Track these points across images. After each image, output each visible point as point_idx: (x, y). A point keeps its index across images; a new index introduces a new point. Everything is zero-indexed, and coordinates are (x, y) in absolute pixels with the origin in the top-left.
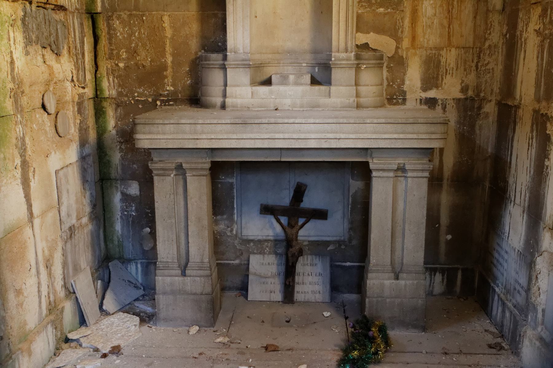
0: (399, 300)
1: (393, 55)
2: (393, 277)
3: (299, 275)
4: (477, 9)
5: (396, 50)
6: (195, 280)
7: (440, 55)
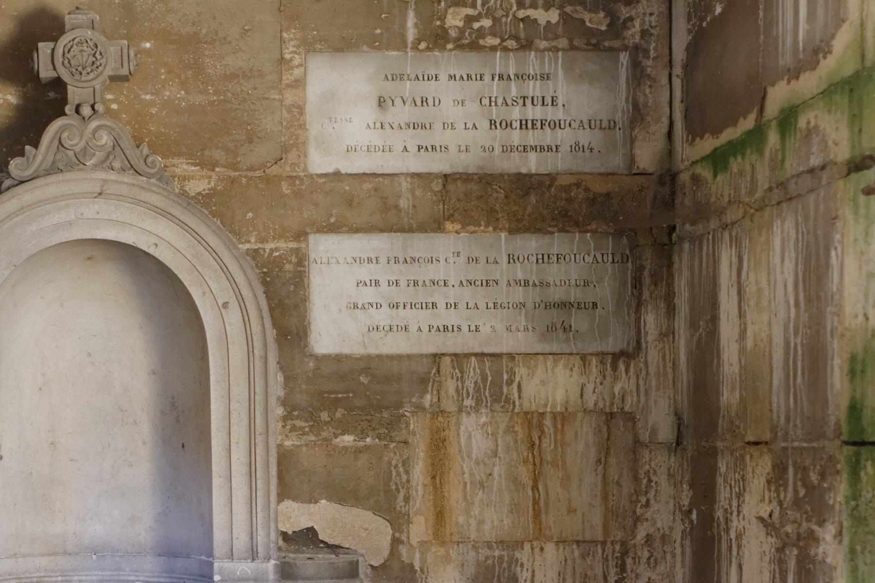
1: (386, 561)
4: (608, 439)
5: (392, 549)
7: (513, 561)
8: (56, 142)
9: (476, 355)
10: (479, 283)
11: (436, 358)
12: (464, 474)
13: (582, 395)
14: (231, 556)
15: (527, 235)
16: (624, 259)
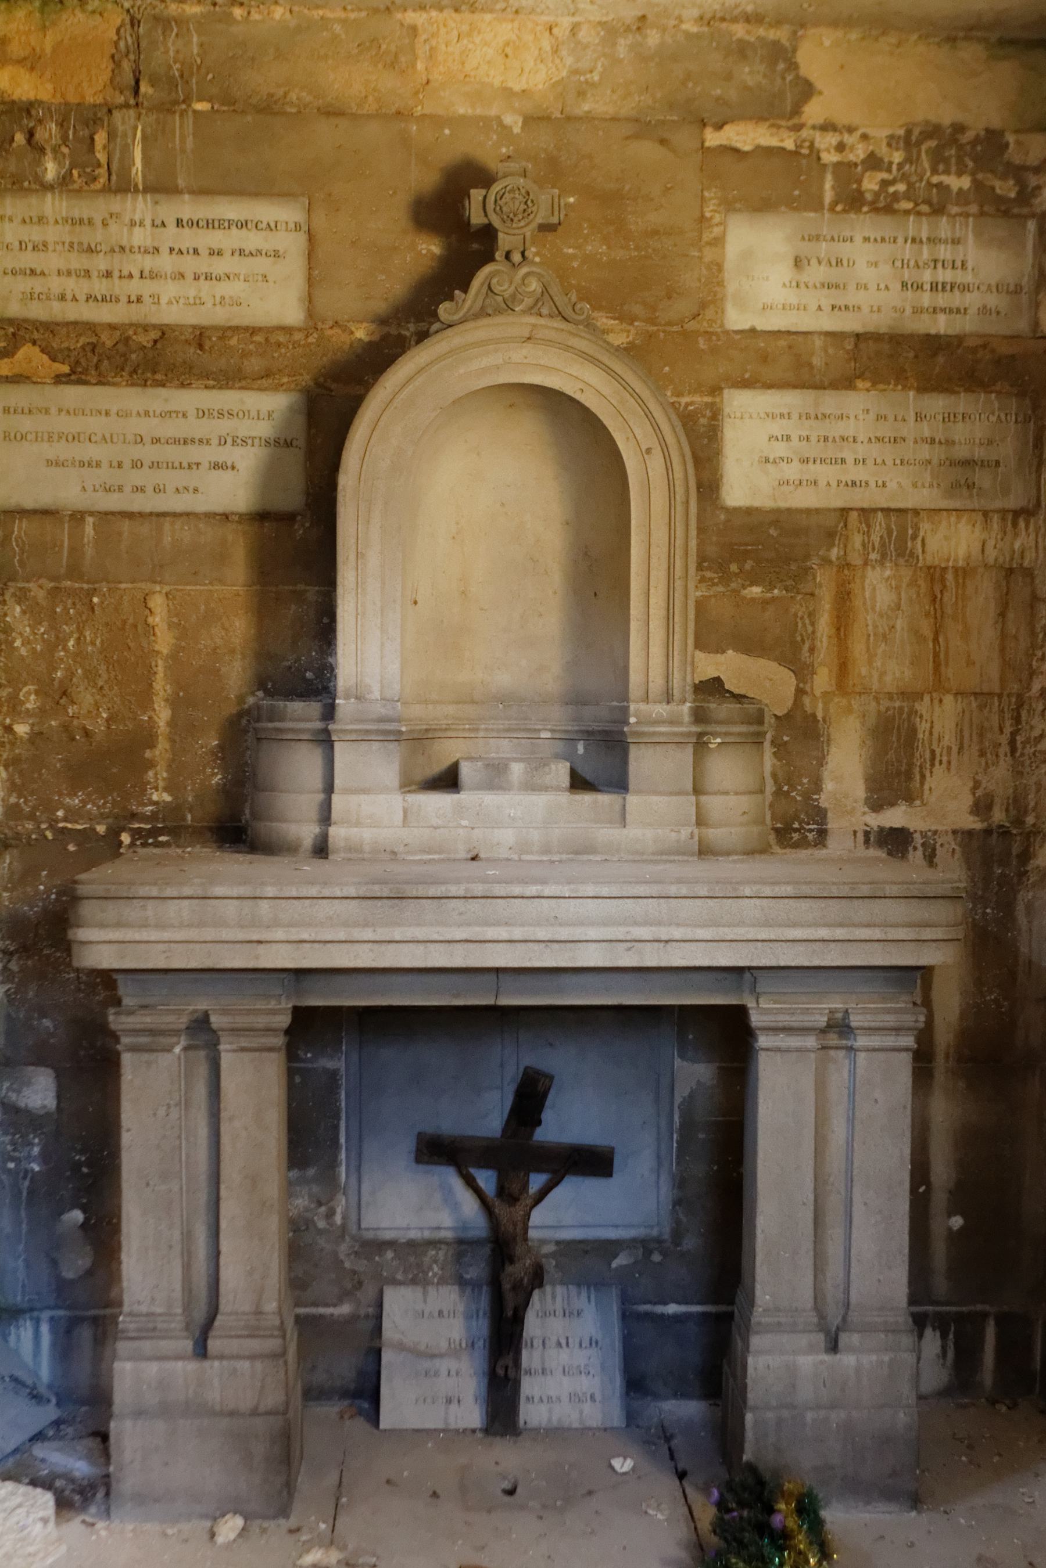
0: (843, 1415)
1: (790, 711)
2: (823, 1345)
3: (532, 1345)
4: (1007, 594)
5: (795, 700)
6: (235, 1370)
7: (913, 712)
8: (486, 287)
9: (882, 510)
10: (887, 440)
11: (844, 512)
12: (867, 625)
13: (983, 551)
14: (646, 699)
15: (934, 395)
16: (1027, 420)
